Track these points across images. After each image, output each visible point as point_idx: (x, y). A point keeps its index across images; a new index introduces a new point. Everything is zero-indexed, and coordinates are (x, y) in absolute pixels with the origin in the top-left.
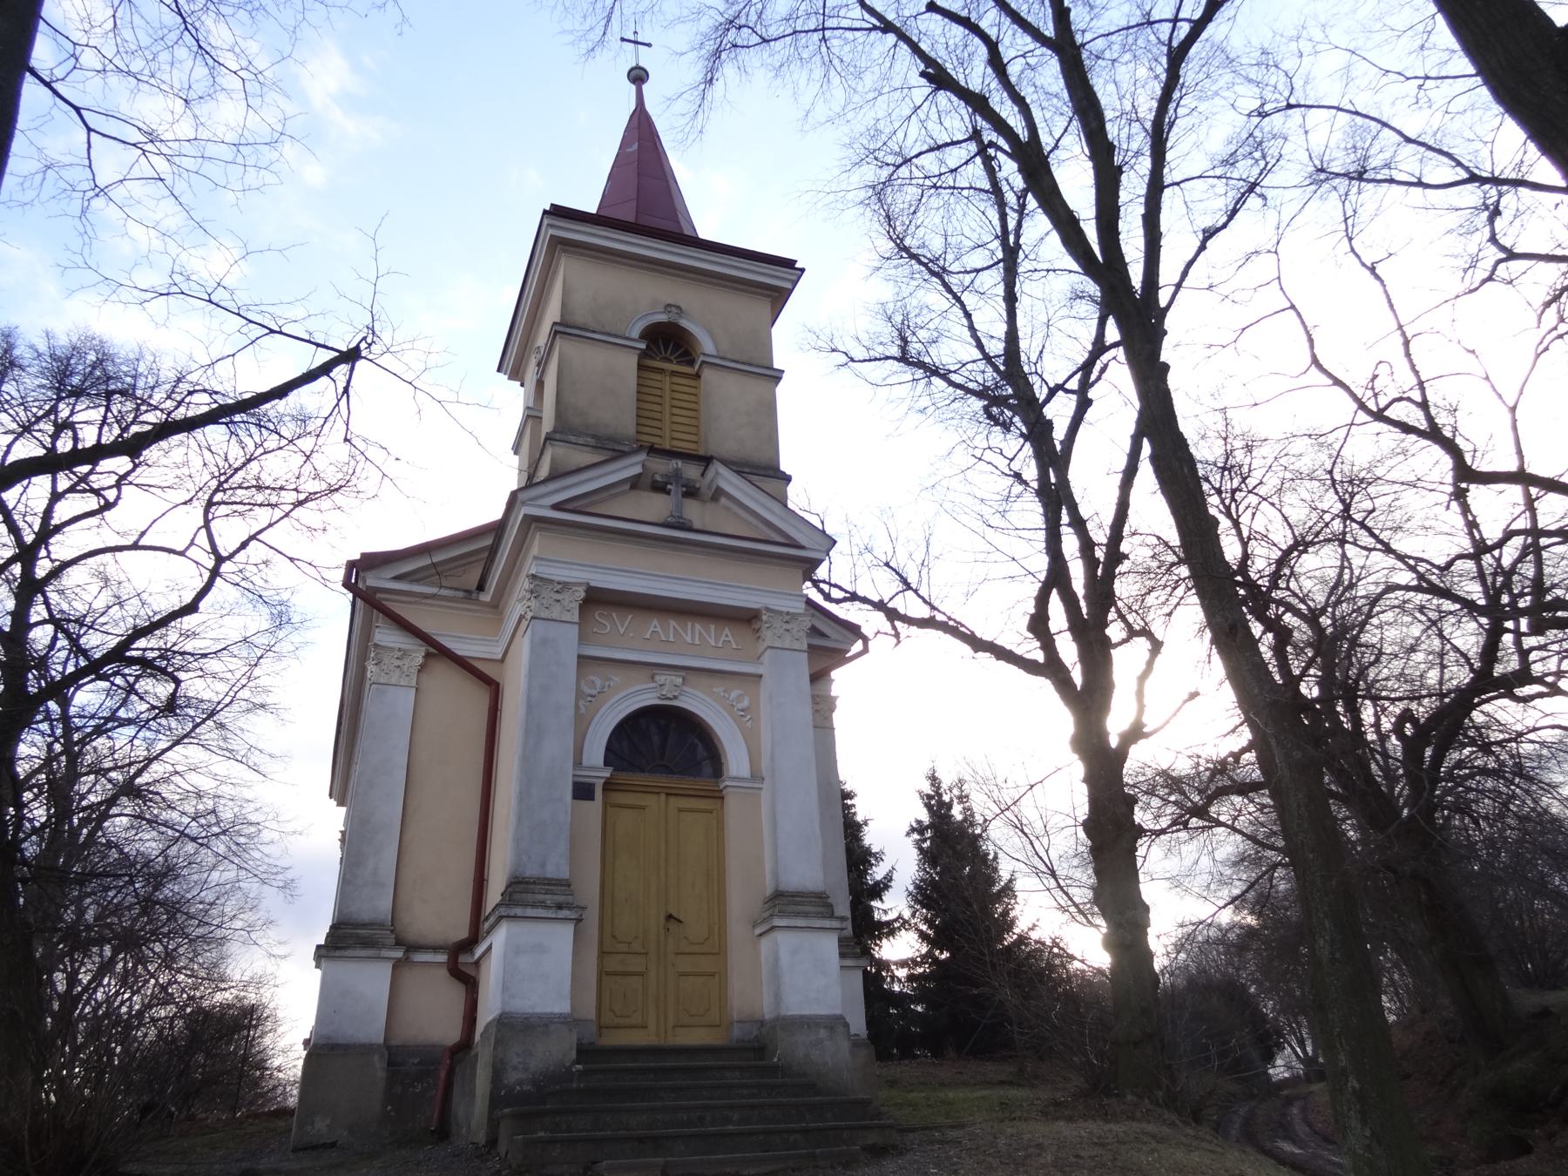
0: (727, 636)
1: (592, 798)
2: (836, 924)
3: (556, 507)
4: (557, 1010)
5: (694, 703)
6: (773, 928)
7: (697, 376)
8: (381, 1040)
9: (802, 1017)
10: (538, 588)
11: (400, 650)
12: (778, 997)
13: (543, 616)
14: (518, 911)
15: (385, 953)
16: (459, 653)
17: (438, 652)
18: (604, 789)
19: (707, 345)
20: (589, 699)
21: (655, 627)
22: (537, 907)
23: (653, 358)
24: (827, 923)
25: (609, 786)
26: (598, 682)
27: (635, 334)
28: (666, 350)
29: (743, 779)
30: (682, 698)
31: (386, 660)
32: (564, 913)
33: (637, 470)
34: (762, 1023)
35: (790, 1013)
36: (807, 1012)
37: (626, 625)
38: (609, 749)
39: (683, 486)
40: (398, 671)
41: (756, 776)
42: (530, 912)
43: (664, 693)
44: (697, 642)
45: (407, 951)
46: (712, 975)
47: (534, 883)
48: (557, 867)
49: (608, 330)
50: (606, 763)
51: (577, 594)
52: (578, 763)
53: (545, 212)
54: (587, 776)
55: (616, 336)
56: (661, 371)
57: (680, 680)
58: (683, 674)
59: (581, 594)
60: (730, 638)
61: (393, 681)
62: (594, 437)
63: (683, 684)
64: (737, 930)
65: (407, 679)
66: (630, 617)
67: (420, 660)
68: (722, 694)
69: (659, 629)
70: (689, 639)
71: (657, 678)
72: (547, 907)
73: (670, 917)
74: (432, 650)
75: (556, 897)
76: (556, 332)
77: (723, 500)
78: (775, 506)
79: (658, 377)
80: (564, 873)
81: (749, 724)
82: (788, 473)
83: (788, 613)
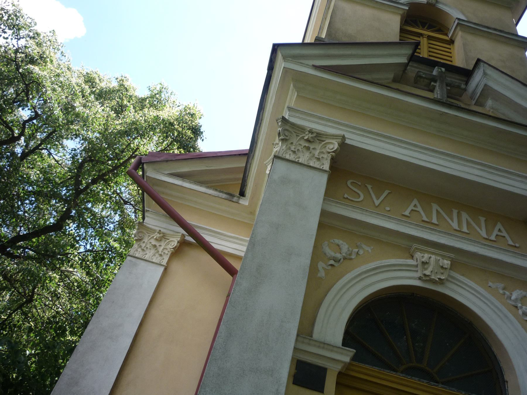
7: (451, 42)
11: (160, 232)
13: (287, 157)
26: (345, 248)
31: (146, 240)
33: (404, 60)
37: (382, 198)
38: (347, 333)
39: (447, 85)
40: (153, 251)
43: (427, 272)
44: (465, 229)
51: (331, 146)
56: (421, 35)
57: (447, 263)
58: (452, 255)
59: (335, 145)
60: (504, 234)
61: (147, 257)
63: (450, 269)
65: (159, 258)
67: (174, 242)
69: (419, 209)
70: (455, 225)
71: (418, 255)
77: (490, 103)
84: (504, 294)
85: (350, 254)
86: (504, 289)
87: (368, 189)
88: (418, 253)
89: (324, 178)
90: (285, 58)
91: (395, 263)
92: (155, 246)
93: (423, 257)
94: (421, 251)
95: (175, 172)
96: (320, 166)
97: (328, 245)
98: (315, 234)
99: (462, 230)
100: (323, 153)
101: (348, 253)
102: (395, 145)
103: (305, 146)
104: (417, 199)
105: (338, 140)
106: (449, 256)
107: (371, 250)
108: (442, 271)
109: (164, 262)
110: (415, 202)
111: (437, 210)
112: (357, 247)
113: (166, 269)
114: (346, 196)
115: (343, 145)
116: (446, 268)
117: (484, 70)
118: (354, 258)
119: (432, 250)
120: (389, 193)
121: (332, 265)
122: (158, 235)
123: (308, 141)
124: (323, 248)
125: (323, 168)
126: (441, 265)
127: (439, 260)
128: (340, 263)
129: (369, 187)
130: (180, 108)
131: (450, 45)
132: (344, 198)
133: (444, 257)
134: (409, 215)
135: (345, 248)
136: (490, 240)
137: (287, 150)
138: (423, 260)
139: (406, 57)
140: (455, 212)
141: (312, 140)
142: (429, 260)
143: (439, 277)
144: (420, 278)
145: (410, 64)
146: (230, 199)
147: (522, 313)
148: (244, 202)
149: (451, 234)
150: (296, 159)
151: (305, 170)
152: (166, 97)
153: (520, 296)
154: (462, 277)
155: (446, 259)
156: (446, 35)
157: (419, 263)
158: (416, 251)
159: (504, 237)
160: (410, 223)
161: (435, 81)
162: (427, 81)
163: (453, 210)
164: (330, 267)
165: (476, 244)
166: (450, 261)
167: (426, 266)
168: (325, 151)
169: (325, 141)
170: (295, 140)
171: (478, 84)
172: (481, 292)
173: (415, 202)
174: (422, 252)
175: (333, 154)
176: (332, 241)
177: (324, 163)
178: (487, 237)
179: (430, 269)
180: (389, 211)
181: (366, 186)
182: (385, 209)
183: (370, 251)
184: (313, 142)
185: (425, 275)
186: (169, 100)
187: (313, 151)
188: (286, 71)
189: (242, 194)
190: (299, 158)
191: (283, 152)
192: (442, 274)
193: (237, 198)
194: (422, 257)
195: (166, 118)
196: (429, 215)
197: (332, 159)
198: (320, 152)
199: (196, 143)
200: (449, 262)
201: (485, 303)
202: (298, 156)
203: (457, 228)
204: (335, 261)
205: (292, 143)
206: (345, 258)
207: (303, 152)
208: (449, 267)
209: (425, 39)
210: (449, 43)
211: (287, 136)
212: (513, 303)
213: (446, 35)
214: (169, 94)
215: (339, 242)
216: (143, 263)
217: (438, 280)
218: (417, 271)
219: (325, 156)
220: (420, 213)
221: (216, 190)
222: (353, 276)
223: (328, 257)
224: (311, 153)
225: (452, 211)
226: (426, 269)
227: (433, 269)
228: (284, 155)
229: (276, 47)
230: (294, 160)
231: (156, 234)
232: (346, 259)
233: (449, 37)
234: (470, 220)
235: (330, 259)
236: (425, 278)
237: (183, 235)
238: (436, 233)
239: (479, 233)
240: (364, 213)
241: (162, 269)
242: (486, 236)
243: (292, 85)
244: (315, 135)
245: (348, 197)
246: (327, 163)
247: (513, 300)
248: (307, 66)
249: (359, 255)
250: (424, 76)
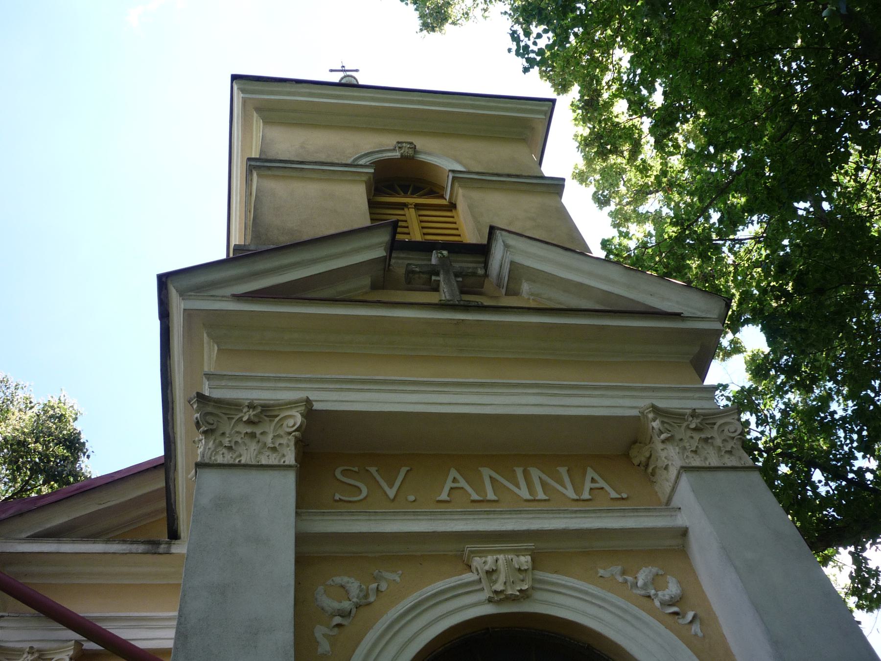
5: (569, 602)
7: (452, 206)
10: (210, 419)
13: (220, 460)
20: (337, 620)
26: (354, 586)
30: (538, 595)
33: (380, 253)
43: (499, 587)
44: (541, 495)
51: (291, 422)
56: (404, 206)
57: (525, 561)
58: (531, 545)
59: (296, 418)
60: (602, 483)
63: (533, 569)
66: (403, 470)
68: (620, 579)
69: (462, 483)
70: (524, 493)
71: (477, 562)
77: (525, 287)
81: (696, 628)
84: (626, 581)
85: (366, 596)
86: (624, 573)
87: (372, 474)
88: (476, 558)
89: (289, 480)
90: (182, 294)
91: (443, 587)
93: (485, 562)
94: (481, 553)
95: (41, 529)
96: (280, 461)
97: (325, 591)
98: (292, 582)
99: (537, 498)
100: (279, 436)
101: (362, 595)
102: (395, 391)
103: (247, 433)
104: (456, 469)
105: (299, 409)
106: (525, 549)
107: (399, 577)
108: (521, 577)
110: (453, 473)
111: (491, 477)
112: (375, 579)
114: (337, 497)
115: (310, 413)
116: (526, 570)
117: (503, 242)
118: (375, 600)
119: (498, 546)
120: (408, 471)
121: (339, 625)
123: (250, 422)
124: (316, 599)
125: (284, 462)
126: (517, 566)
127: (512, 560)
128: (351, 618)
129: (373, 470)
130: (35, 410)
131: (451, 211)
132: (336, 501)
133: (518, 552)
134: (448, 499)
135: (354, 586)
136: (584, 500)
137: (216, 447)
138: (487, 568)
139: (383, 248)
140: (519, 472)
141: (256, 420)
142: (496, 566)
143: (519, 588)
144: (490, 600)
145: (394, 255)
146: (153, 551)
147: (659, 604)
148: (180, 548)
149: (521, 511)
150: (235, 459)
151: (254, 474)
152: (7, 396)
153: (649, 578)
154: (555, 576)
155: (523, 554)
156: (442, 197)
157: (483, 575)
158: (472, 556)
159: (602, 488)
160: (451, 513)
161: (438, 274)
162: (424, 276)
163: (515, 468)
164: (336, 629)
165: (562, 515)
166: (530, 555)
167: (494, 577)
168: (282, 433)
169: (278, 416)
170: (227, 427)
171: (502, 263)
172: (590, 590)
173: (453, 473)
174: (480, 555)
175: (297, 433)
176: (330, 582)
177: (285, 454)
178: (578, 498)
179: (502, 579)
180: (414, 501)
181: (367, 471)
182: (407, 500)
183: (398, 579)
184: (259, 422)
185: (496, 592)
186: (15, 399)
187: (262, 438)
188: (189, 314)
189: (174, 535)
190: (240, 456)
191: (209, 453)
192: (523, 581)
193: (166, 546)
194: (484, 563)
195: (9, 435)
196: (480, 489)
197: (298, 442)
198: (274, 436)
199: (78, 465)
200: (529, 558)
201: (600, 607)
202: (237, 453)
203: (529, 497)
204: (342, 617)
205: (223, 434)
206: (358, 606)
207: (245, 444)
208: (530, 565)
209: (412, 211)
210: (450, 209)
211: (213, 424)
212: (643, 592)
213: (442, 197)
214: (12, 389)
215: (342, 580)
217: (518, 593)
218: (482, 589)
219: (284, 441)
220: (465, 489)
221: (124, 542)
222: (378, 634)
223: (329, 613)
224: (259, 442)
225: (514, 471)
226: (495, 582)
227: (506, 577)
228: (213, 458)
229: (164, 279)
230: (231, 462)
231: (25, 656)
232: (360, 606)
233: (446, 199)
234: (545, 477)
235: (333, 615)
236: (498, 597)
237: (78, 643)
238: (496, 516)
239: (564, 494)
240: (372, 518)
242: (575, 497)
243: (205, 335)
244: (259, 410)
245: (342, 498)
246: (289, 452)
247: (642, 588)
248: (223, 298)
249: (382, 592)
250: (417, 269)
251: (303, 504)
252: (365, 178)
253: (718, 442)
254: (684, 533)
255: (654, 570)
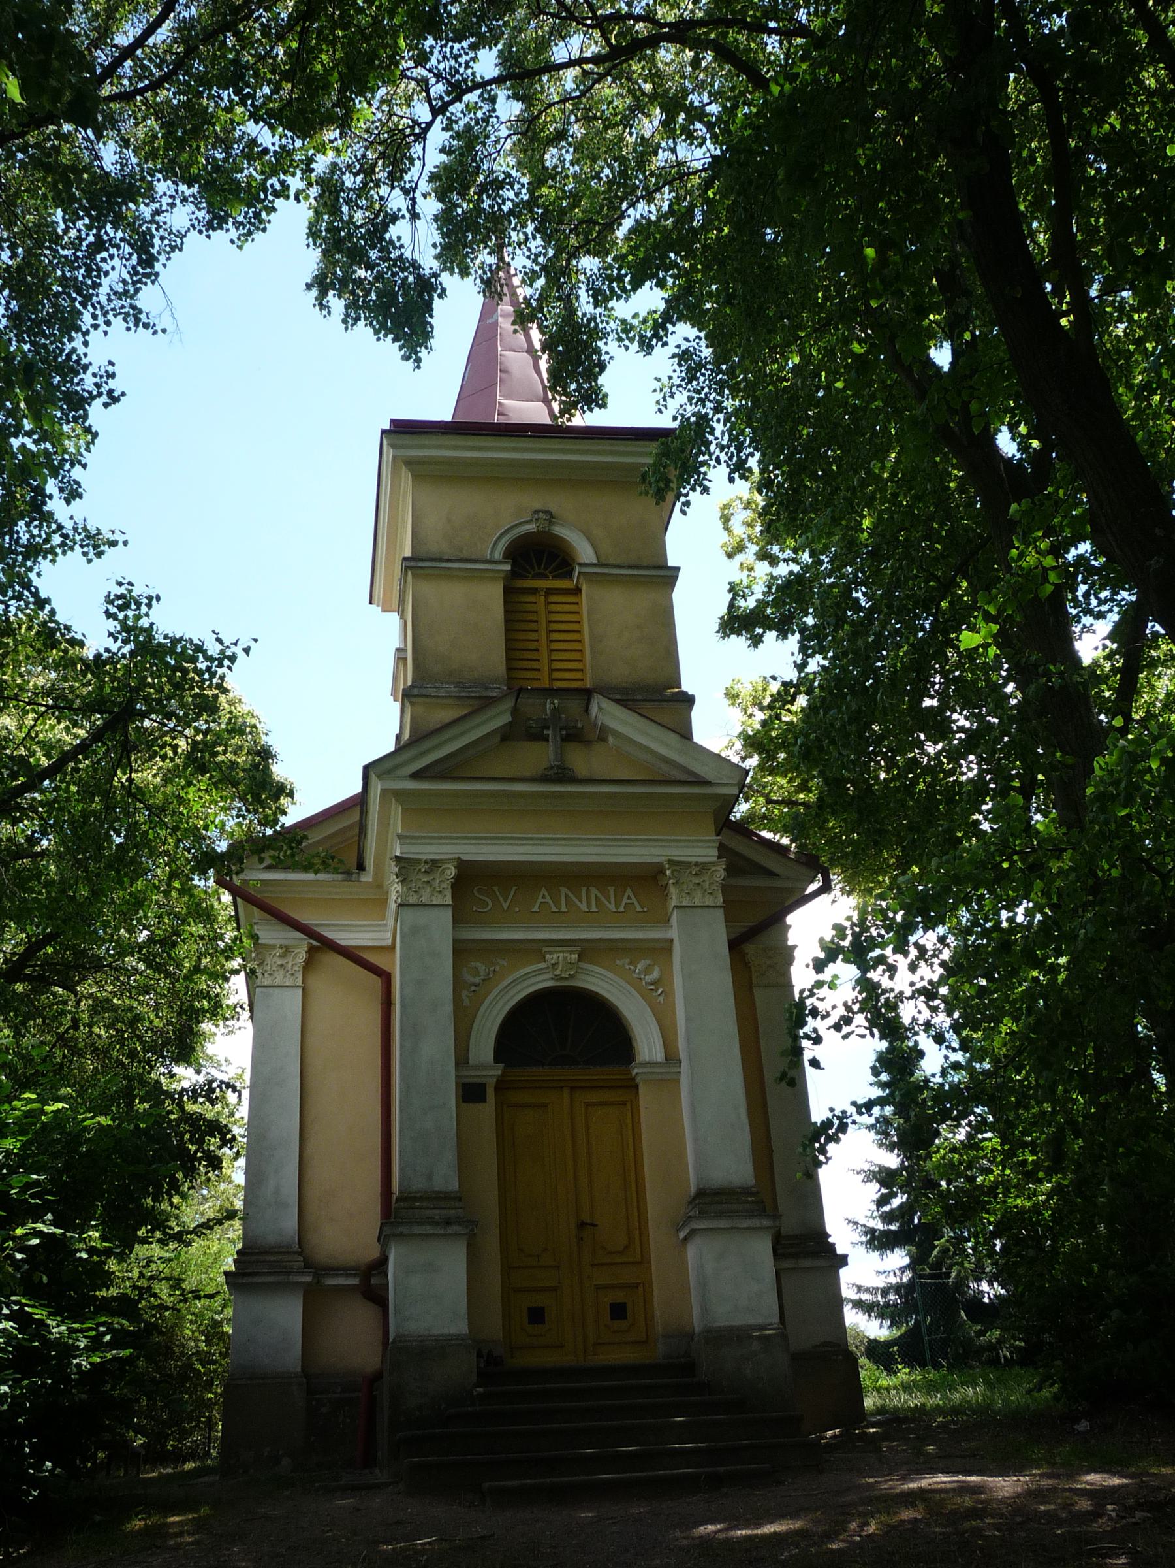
0: (629, 898)
1: (483, 1099)
2: (766, 1223)
3: (416, 776)
4: (453, 1331)
6: (693, 1232)
7: (577, 591)
8: (299, 1369)
9: (731, 1329)
12: (704, 1309)
14: (405, 1230)
15: (293, 1279)
16: (342, 943)
17: (322, 946)
18: (496, 1089)
19: (585, 552)
20: (473, 988)
21: (544, 897)
22: (423, 1223)
23: (526, 577)
24: (756, 1223)
25: (502, 1086)
27: (498, 554)
28: (539, 565)
29: (655, 1064)
30: (579, 976)
31: (268, 961)
32: (451, 1230)
33: (506, 718)
34: (691, 1336)
35: (718, 1324)
36: (736, 1323)
39: (561, 729)
40: (282, 972)
41: (671, 1058)
42: (417, 1230)
43: (558, 972)
45: (316, 1275)
46: (637, 1286)
47: (420, 1199)
48: (445, 1178)
49: (466, 554)
50: (498, 1058)
52: (462, 1060)
53: (383, 432)
54: (472, 1075)
55: (475, 561)
56: (534, 591)
57: (575, 956)
59: (451, 872)
60: (634, 900)
61: (277, 982)
62: (460, 685)
64: (658, 1236)
67: (303, 956)
69: (548, 899)
70: (584, 907)
71: (548, 957)
72: (435, 1223)
73: (582, 1225)
74: (314, 943)
75: (445, 1211)
76: (407, 568)
77: (611, 739)
78: (673, 739)
79: (531, 599)
80: (454, 1185)
81: (661, 999)
82: (690, 693)
83: (696, 864)
92: (282, 965)
94: (551, 953)
109: (299, 982)
110: (544, 891)
113: (304, 989)
122: (279, 952)
133: (571, 952)
135: (482, 968)
140: (584, 890)
148: (367, 877)
161: (548, 728)
173: (544, 891)
189: (361, 867)
196: (557, 903)
216: (277, 990)
234: (599, 895)
236: (558, 978)
241: (300, 991)
251: (456, 921)
252: (502, 575)
253: (707, 885)
254: (672, 941)
255: (648, 962)
